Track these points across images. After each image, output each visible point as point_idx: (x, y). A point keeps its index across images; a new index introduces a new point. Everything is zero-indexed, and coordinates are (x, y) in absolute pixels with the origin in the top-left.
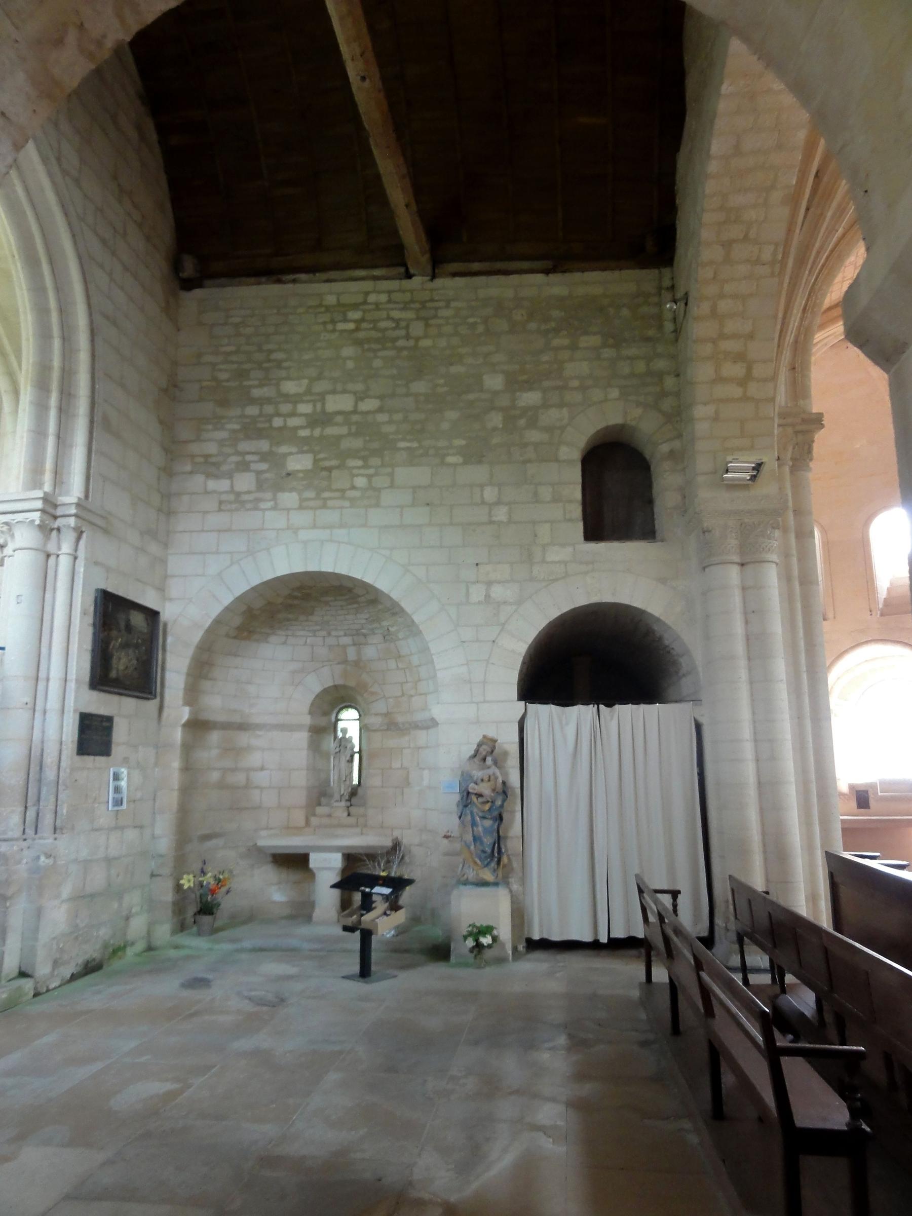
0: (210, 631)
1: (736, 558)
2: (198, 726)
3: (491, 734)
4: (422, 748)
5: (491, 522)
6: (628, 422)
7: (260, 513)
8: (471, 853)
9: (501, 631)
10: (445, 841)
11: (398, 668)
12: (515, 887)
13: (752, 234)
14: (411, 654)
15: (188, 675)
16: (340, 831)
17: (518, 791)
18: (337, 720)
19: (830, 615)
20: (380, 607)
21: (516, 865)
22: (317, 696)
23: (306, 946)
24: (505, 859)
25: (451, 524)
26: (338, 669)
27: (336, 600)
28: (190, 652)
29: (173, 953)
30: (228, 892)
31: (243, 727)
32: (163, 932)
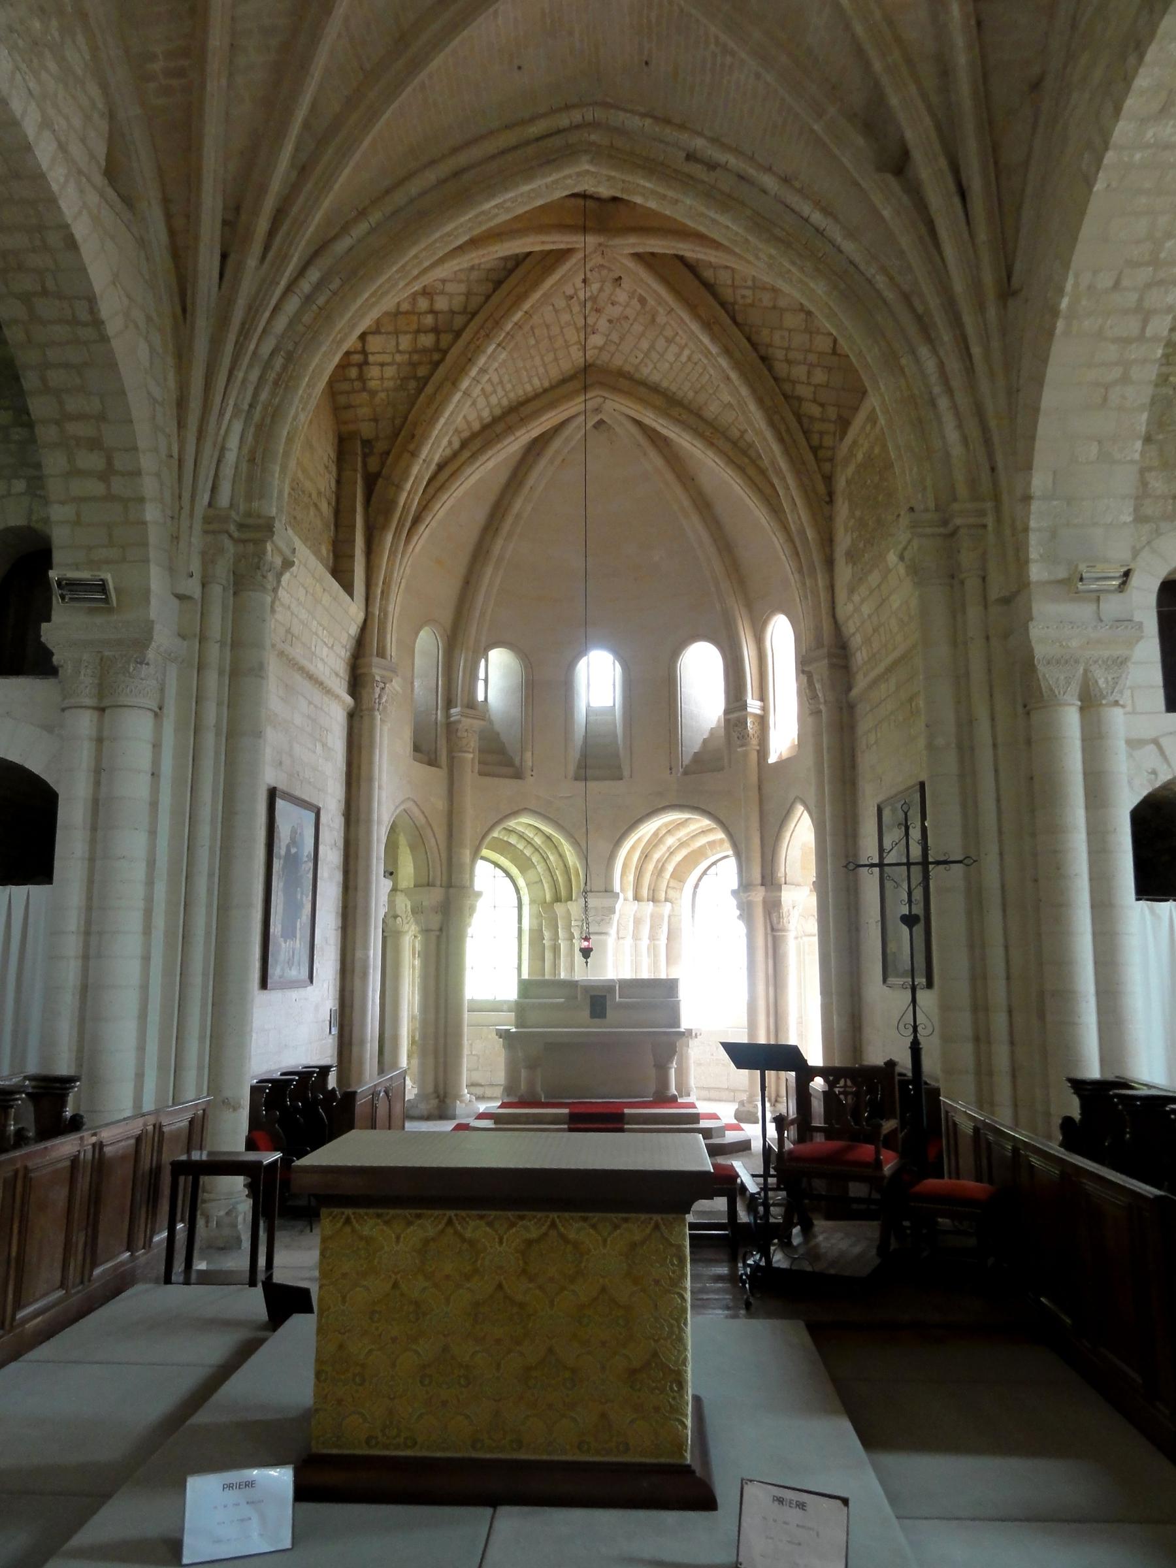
1: (89, 702)
6: (33, 524)
13: (50, 285)
19: (626, 773)
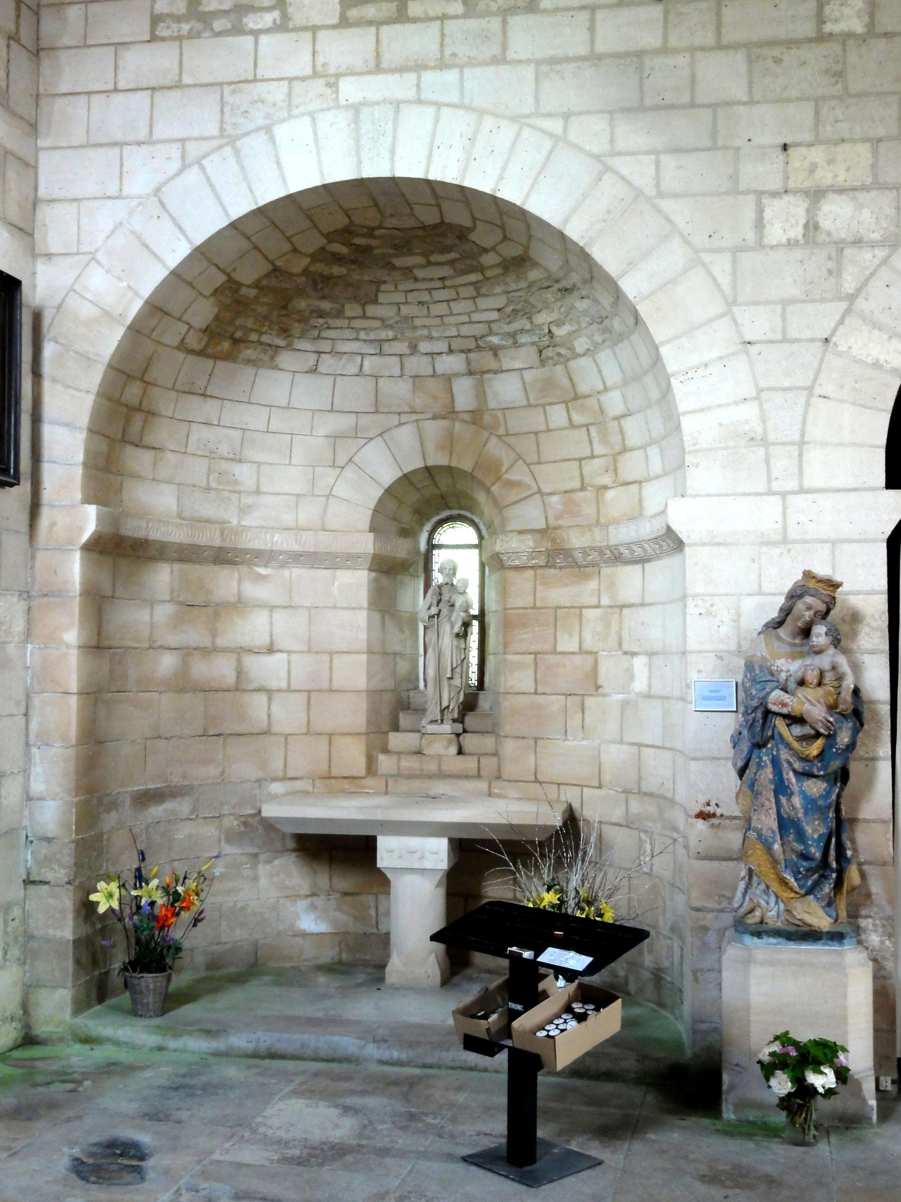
0: (136, 330)
2: (119, 551)
4: (631, 606)
5: (822, 38)
7: (249, 40)
8: (775, 862)
9: (848, 312)
10: (701, 824)
11: (572, 426)
12: (874, 939)
14: (606, 389)
15: (92, 431)
16: (441, 788)
17: (886, 709)
18: (432, 546)
20: (534, 275)
21: (876, 887)
22: (389, 491)
23: (372, 1051)
24: (853, 875)
25: (720, 46)
26: (434, 429)
27: (429, 264)
28: (94, 378)
29: (77, 1056)
30: (197, 921)
31: (224, 557)
32: (56, 1006)
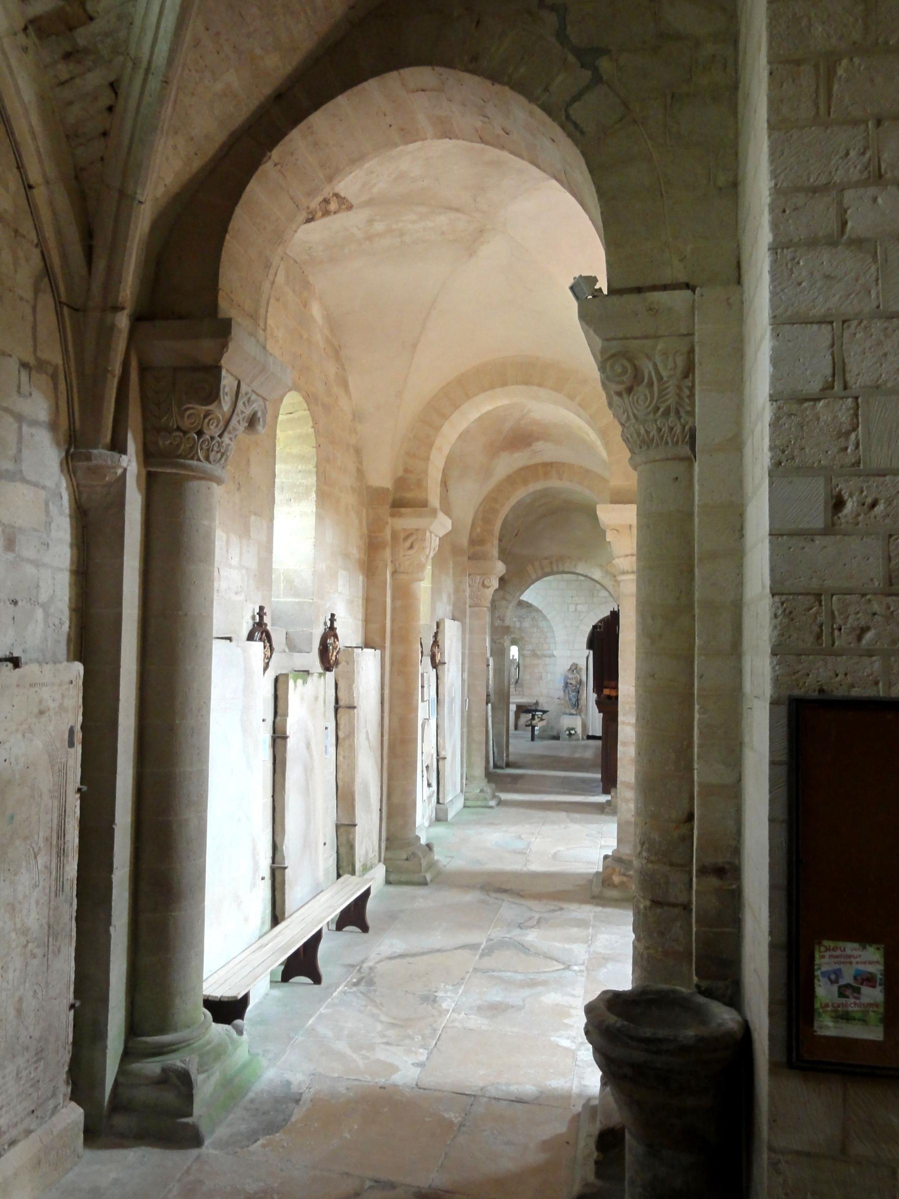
3: (576, 662)
21: (584, 709)
